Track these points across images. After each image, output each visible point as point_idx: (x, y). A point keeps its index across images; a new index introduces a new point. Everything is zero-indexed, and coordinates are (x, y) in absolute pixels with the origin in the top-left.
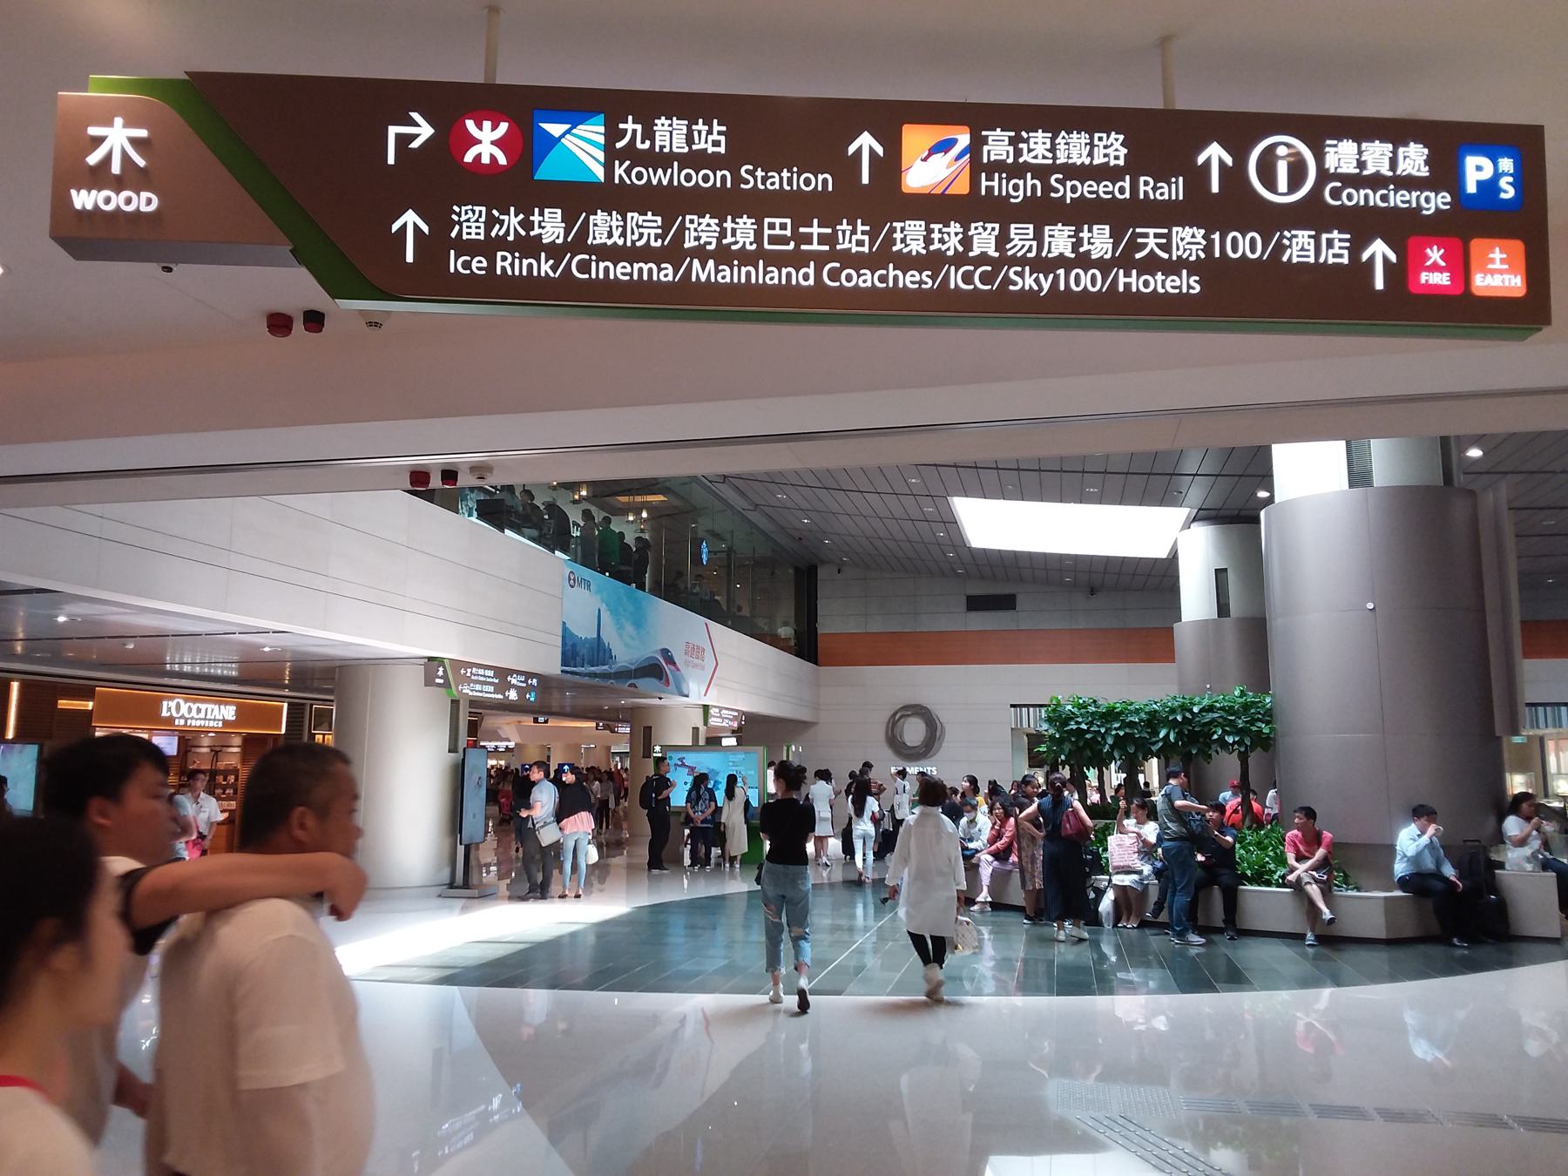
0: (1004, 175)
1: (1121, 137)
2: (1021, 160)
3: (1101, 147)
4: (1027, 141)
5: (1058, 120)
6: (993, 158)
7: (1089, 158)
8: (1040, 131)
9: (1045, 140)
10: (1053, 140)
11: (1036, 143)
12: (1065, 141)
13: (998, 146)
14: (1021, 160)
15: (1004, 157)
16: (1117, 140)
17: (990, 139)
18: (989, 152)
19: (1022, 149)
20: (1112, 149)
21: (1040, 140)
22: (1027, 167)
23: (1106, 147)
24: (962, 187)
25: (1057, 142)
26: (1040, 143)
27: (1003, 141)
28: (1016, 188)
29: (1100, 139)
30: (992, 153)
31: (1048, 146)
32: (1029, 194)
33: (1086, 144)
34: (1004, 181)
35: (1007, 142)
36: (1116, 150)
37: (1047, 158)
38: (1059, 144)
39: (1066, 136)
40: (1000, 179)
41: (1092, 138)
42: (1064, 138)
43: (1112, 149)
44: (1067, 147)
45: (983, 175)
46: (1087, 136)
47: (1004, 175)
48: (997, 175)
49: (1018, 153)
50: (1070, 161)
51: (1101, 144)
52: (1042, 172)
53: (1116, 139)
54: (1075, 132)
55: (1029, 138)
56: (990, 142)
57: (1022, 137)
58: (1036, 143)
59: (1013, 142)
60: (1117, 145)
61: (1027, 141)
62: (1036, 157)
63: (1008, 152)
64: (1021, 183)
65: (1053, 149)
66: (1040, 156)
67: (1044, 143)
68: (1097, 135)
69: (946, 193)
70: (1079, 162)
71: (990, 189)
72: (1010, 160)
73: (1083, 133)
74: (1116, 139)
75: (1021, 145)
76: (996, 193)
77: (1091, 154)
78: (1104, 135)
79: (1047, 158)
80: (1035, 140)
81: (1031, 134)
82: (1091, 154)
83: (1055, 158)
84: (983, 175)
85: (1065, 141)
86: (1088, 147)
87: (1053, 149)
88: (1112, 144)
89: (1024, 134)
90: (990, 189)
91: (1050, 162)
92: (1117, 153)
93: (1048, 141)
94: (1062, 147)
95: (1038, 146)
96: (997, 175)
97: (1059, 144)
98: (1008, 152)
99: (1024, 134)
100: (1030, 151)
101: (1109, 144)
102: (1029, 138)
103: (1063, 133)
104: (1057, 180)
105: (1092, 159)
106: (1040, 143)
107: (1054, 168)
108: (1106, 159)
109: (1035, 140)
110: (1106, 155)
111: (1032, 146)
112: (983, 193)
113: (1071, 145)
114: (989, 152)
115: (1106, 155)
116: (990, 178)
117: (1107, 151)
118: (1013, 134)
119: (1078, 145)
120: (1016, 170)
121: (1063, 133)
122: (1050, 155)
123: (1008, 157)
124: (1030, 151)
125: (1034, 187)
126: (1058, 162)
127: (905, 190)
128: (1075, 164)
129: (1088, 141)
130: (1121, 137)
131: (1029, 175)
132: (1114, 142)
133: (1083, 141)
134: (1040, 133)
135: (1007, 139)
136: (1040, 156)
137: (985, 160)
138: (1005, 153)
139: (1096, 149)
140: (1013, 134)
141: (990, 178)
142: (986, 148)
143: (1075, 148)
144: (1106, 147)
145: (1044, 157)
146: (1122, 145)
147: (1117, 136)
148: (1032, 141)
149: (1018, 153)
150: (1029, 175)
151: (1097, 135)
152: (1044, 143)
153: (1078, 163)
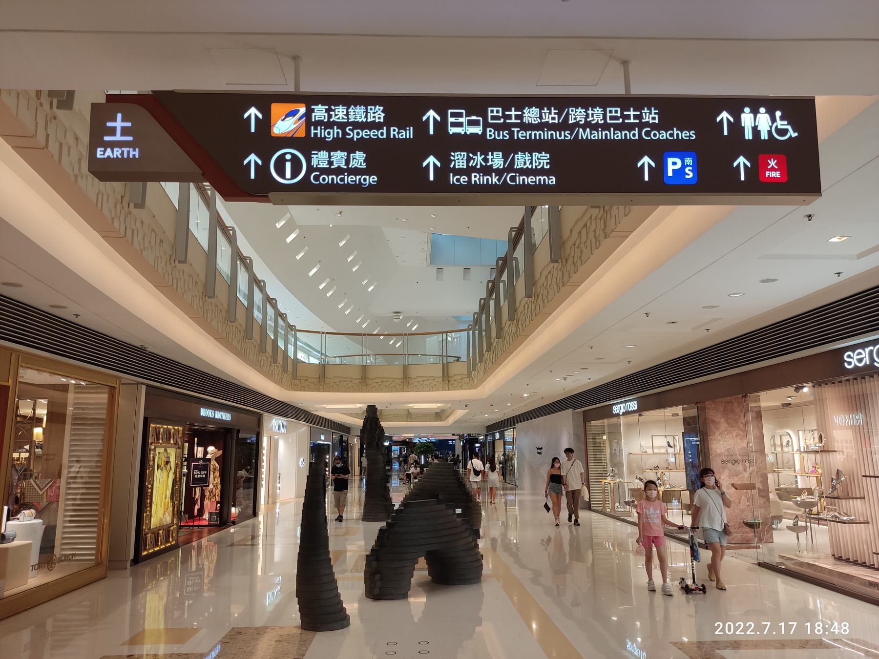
0: (323, 127)
1: (382, 108)
2: (331, 120)
3: (372, 113)
4: (334, 111)
5: (349, 100)
6: (317, 119)
7: (365, 119)
8: (341, 106)
9: (343, 110)
10: (347, 110)
11: (338, 112)
12: (353, 110)
13: (320, 112)
14: (331, 120)
15: (323, 119)
16: (379, 109)
17: (316, 110)
18: (315, 116)
19: (332, 115)
20: (377, 114)
21: (341, 110)
22: (335, 123)
23: (374, 113)
24: (302, 134)
25: (349, 111)
26: (341, 112)
27: (322, 111)
28: (329, 133)
29: (371, 109)
30: (317, 117)
31: (345, 113)
32: (335, 136)
33: (364, 112)
34: (323, 131)
35: (324, 111)
36: (379, 114)
37: (345, 119)
38: (350, 112)
39: (354, 108)
40: (321, 129)
41: (367, 109)
42: (353, 109)
43: (377, 114)
44: (354, 113)
45: (312, 127)
46: (364, 108)
47: (323, 127)
48: (319, 127)
49: (330, 116)
50: (356, 120)
51: (372, 112)
52: (342, 126)
53: (379, 109)
54: (358, 106)
55: (335, 109)
56: (316, 111)
57: (332, 109)
58: (338, 112)
59: (327, 111)
60: (379, 112)
61: (334, 111)
62: (339, 118)
63: (325, 116)
64: (331, 131)
65: (347, 114)
66: (341, 118)
67: (343, 112)
68: (369, 107)
69: (294, 136)
70: (360, 121)
71: (316, 134)
72: (326, 120)
73: (362, 106)
74: (379, 109)
75: (331, 113)
76: (319, 136)
77: (366, 117)
78: (373, 107)
79: (345, 119)
80: (338, 110)
81: (336, 107)
82: (366, 117)
83: (348, 119)
84: (312, 127)
85: (353, 110)
86: (365, 113)
87: (347, 114)
88: (377, 112)
89: (333, 107)
90: (316, 134)
91: (346, 120)
92: (379, 116)
93: (345, 111)
94: (352, 113)
95: (340, 113)
96: (319, 127)
97: (350, 112)
98: (325, 116)
99: (333, 107)
100: (336, 115)
101: (375, 111)
102: (335, 109)
103: (352, 106)
104: (349, 130)
105: (367, 119)
106: (341, 112)
107: (348, 124)
108: (374, 119)
109: (338, 110)
110: (374, 117)
111: (337, 113)
112: (312, 136)
113: (356, 112)
114: (315, 116)
115: (374, 117)
116: (316, 129)
117: (375, 115)
118: (327, 107)
119: (360, 112)
120: (329, 125)
121: (352, 106)
122: (346, 117)
123: (325, 119)
124: (336, 115)
125: (338, 133)
126: (350, 121)
127: (272, 135)
128: (358, 121)
129: (365, 110)
130: (382, 108)
131: (335, 127)
132: (378, 111)
133: (362, 110)
134: (341, 107)
135: (324, 110)
136: (341, 118)
137: (313, 120)
138: (323, 117)
139: (369, 114)
140: (327, 107)
141: (316, 129)
142: (313, 114)
143: (358, 114)
144: (374, 113)
145: (343, 118)
146: (382, 112)
147: (380, 108)
148: (337, 110)
149: (330, 116)
150: (335, 127)
151: (369, 107)
152: (343, 112)
153: (360, 121)
